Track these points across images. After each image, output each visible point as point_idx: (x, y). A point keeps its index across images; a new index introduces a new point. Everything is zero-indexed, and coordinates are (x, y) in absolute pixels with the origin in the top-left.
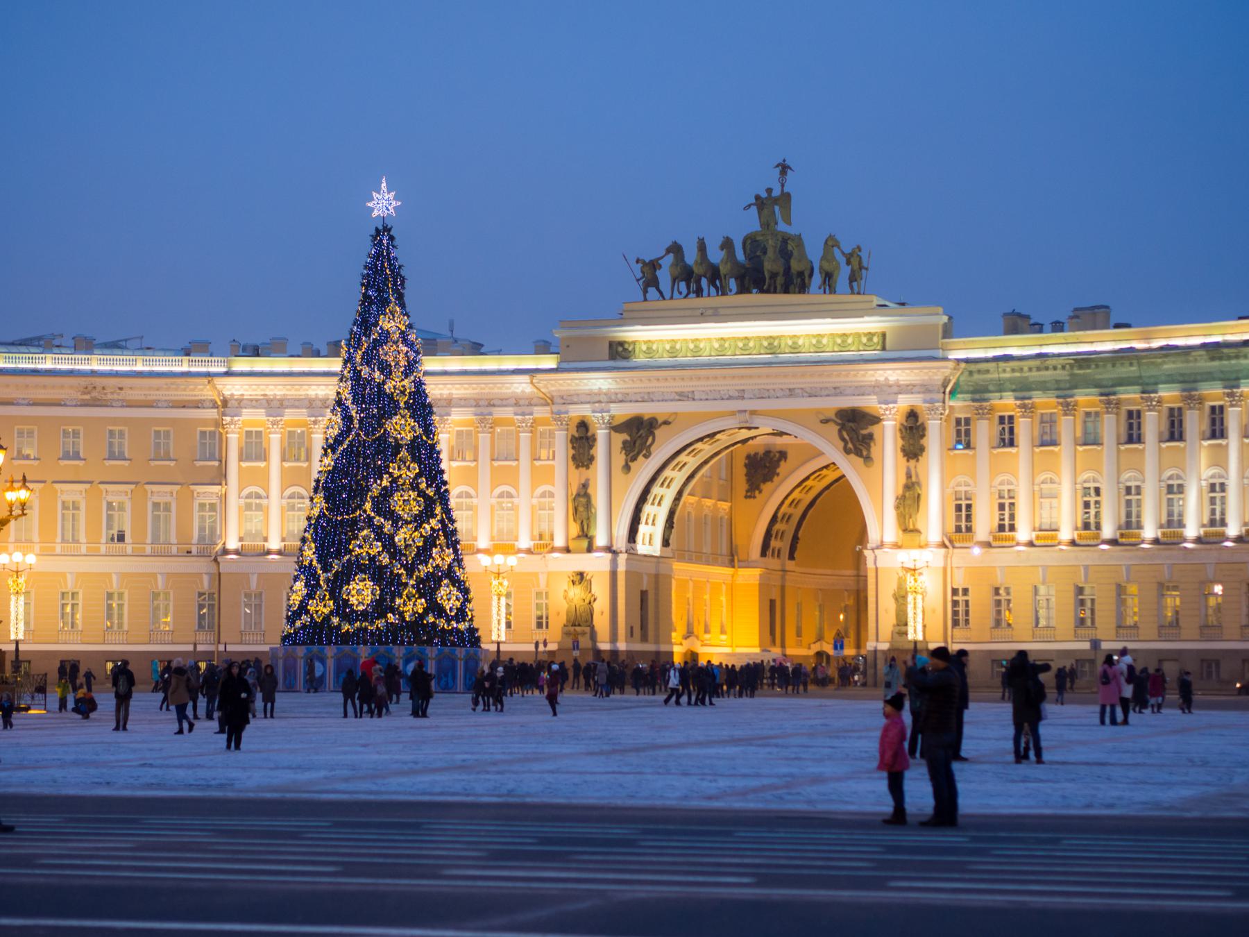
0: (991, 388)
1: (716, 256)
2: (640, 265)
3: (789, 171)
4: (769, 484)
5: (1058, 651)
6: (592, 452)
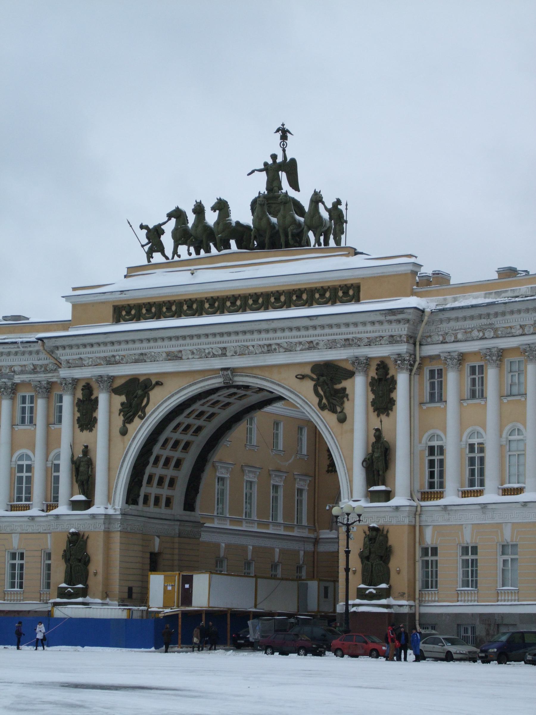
0: (460, 336)
1: (211, 218)
2: (145, 231)
3: (288, 135)
5: (520, 615)
6: (94, 415)
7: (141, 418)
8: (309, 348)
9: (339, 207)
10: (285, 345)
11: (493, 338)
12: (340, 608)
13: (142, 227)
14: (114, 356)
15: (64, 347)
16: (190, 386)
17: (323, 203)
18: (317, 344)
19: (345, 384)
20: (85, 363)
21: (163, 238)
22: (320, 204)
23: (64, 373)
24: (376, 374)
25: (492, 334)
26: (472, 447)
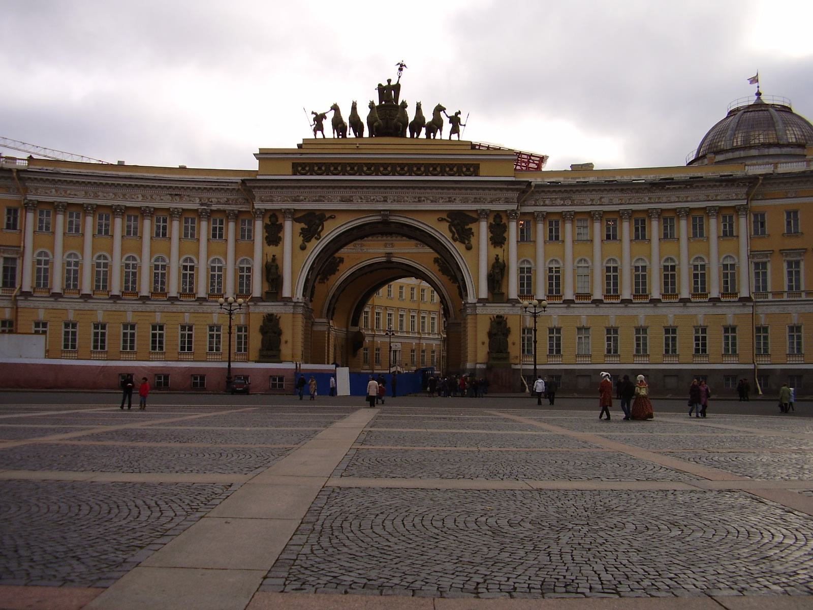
0: (547, 202)
2: (315, 116)
3: (404, 68)
4: (332, 276)
6: (280, 235)
7: (318, 239)
8: (450, 201)
9: (459, 116)
10: (431, 198)
11: (570, 205)
12: (469, 365)
13: (313, 113)
14: (298, 196)
15: (260, 188)
16: (356, 220)
17: (444, 112)
18: (455, 199)
19: (470, 226)
20: (275, 199)
21: (324, 122)
22: (442, 113)
23: (258, 205)
24: (494, 221)
25: (570, 203)
26: (550, 270)
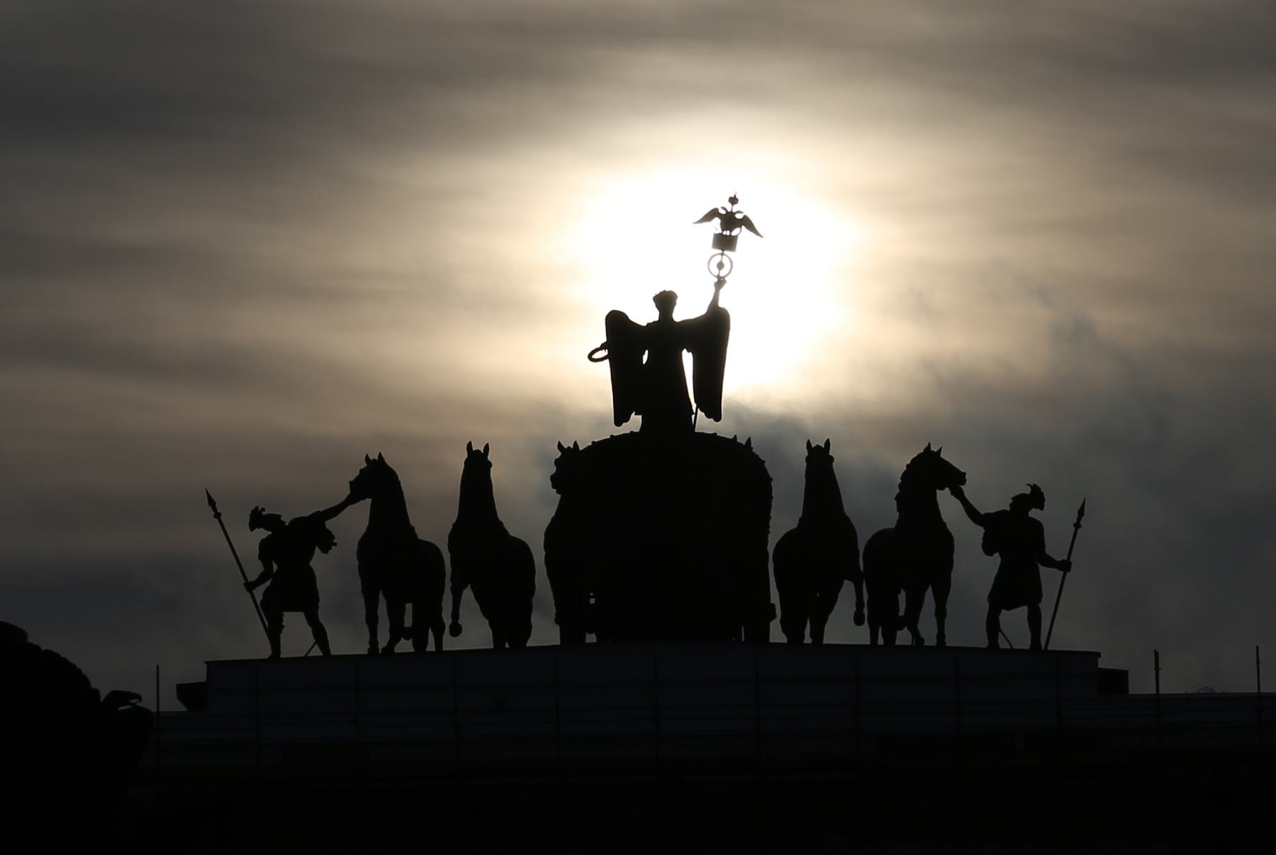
2: (262, 533)
9: (1034, 513)
13: (258, 519)
21: (319, 561)
22: (945, 498)
